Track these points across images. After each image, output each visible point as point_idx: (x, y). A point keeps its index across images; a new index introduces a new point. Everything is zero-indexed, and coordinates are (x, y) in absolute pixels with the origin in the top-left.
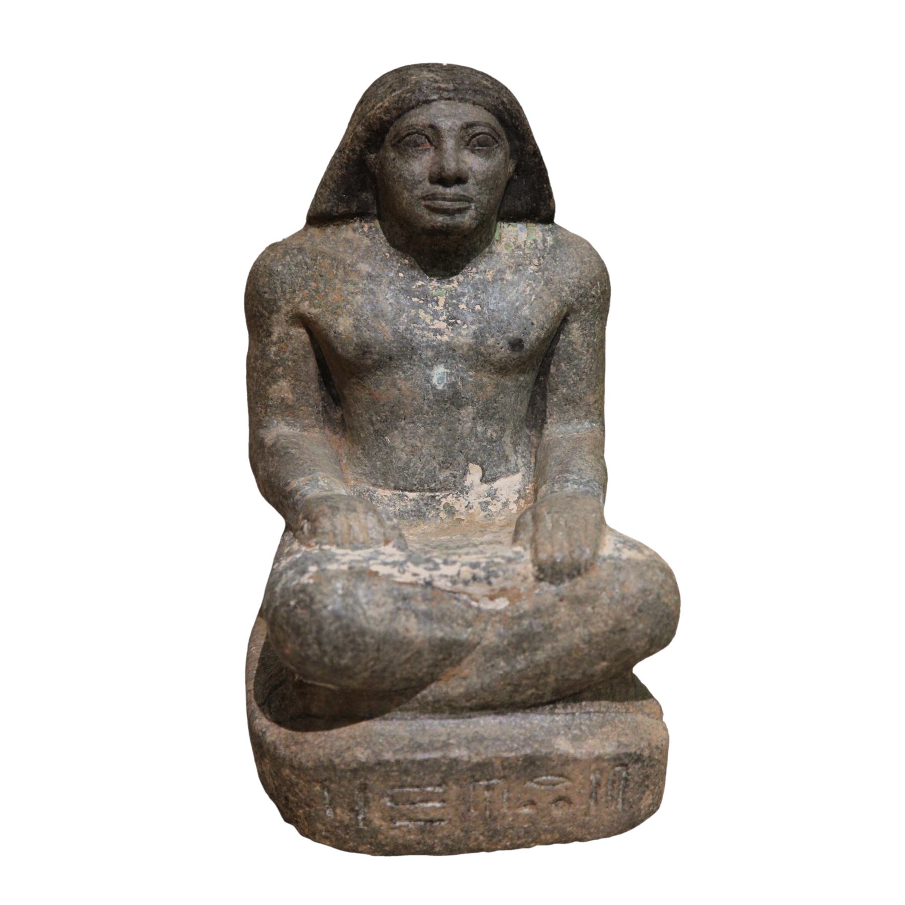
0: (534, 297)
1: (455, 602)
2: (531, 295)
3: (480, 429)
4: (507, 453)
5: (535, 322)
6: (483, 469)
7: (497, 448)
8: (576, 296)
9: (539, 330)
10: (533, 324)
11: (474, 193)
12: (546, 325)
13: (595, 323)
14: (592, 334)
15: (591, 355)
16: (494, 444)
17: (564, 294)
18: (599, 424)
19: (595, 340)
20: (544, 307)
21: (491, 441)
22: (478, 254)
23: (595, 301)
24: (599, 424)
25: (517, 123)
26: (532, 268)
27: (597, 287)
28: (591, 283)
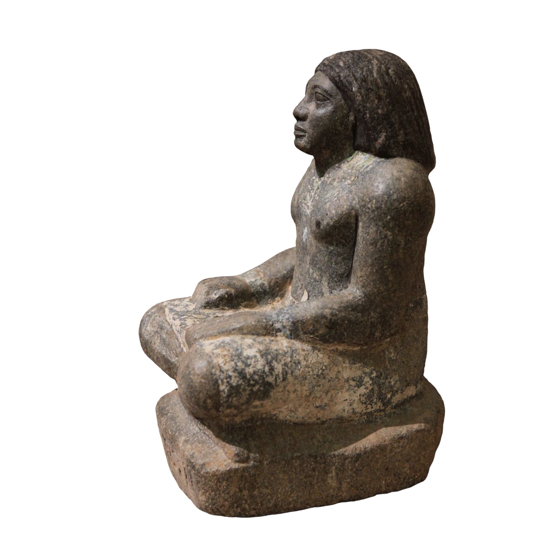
0: (336, 199)
1: (177, 341)
2: (335, 197)
3: (311, 271)
4: (323, 291)
5: (328, 214)
6: (308, 295)
7: (318, 286)
8: (360, 205)
9: (329, 219)
10: (327, 214)
11: (307, 127)
12: (335, 218)
13: (370, 226)
14: (367, 233)
15: (364, 245)
16: (317, 283)
17: (354, 202)
18: (360, 291)
19: (368, 237)
20: (337, 206)
21: (315, 281)
22: (331, 167)
23: (370, 212)
24: (360, 291)
25: (346, 90)
26: (349, 182)
27: (373, 203)
28: (369, 199)
